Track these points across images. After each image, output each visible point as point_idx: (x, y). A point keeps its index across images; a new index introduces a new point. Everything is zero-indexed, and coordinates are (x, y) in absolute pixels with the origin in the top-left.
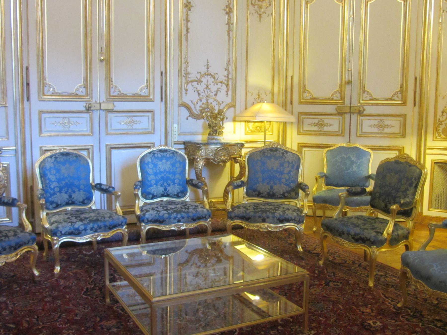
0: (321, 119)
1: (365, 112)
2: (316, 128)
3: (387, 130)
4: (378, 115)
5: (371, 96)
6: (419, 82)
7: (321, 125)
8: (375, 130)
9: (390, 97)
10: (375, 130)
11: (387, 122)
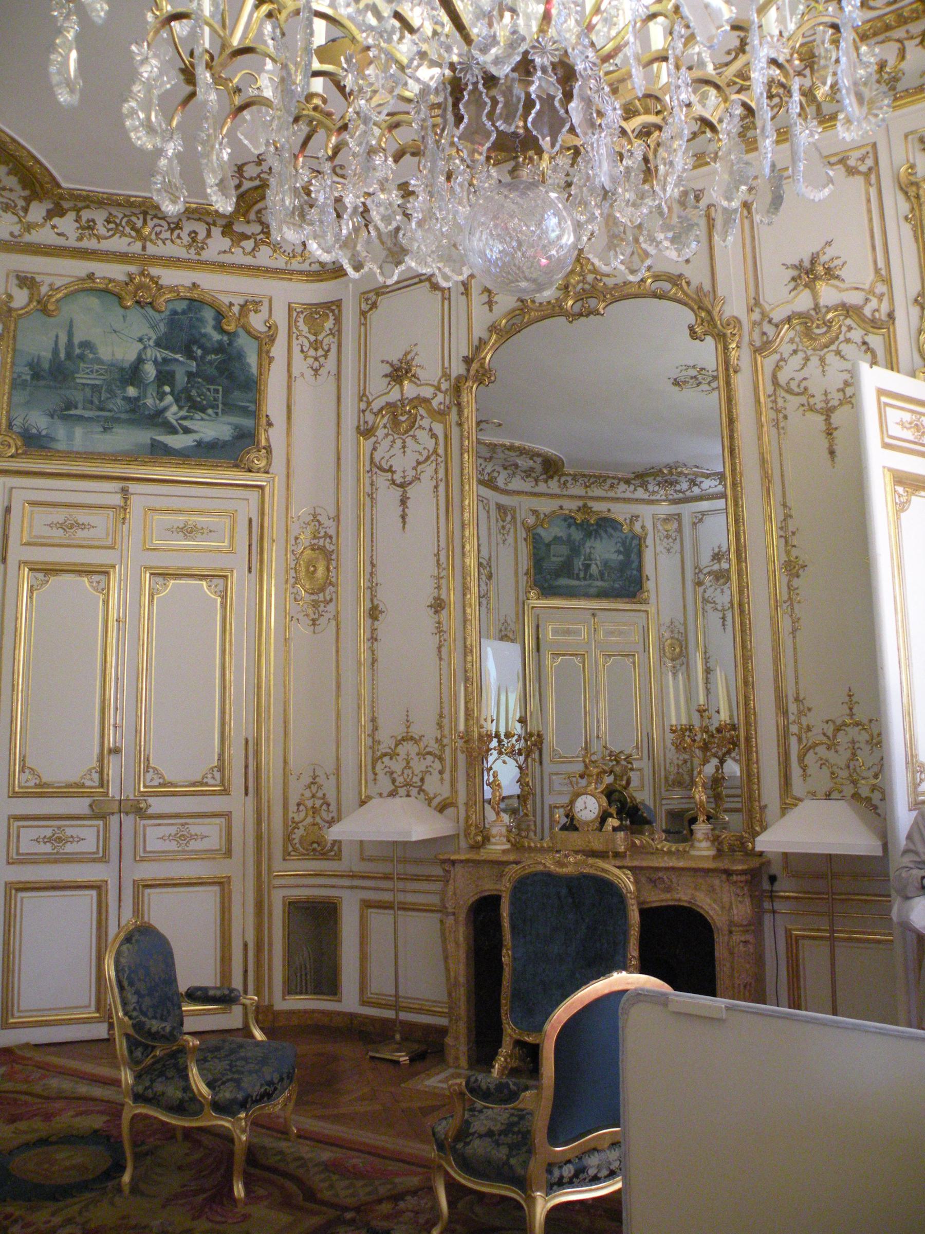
0: (59, 828)
1: (150, 811)
2: (47, 848)
3: (194, 845)
4: (177, 816)
5: (162, 777)
6: (252, 748)
7: (59, 839)
8: (173, 846)
9: (199, 778)
10: (173, 846)
11: (194, 830)
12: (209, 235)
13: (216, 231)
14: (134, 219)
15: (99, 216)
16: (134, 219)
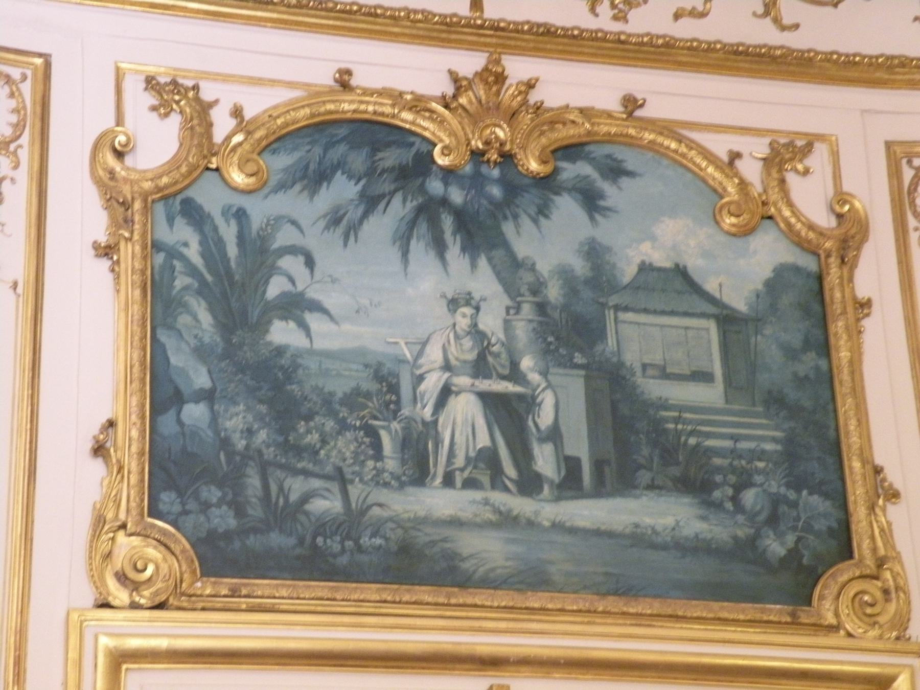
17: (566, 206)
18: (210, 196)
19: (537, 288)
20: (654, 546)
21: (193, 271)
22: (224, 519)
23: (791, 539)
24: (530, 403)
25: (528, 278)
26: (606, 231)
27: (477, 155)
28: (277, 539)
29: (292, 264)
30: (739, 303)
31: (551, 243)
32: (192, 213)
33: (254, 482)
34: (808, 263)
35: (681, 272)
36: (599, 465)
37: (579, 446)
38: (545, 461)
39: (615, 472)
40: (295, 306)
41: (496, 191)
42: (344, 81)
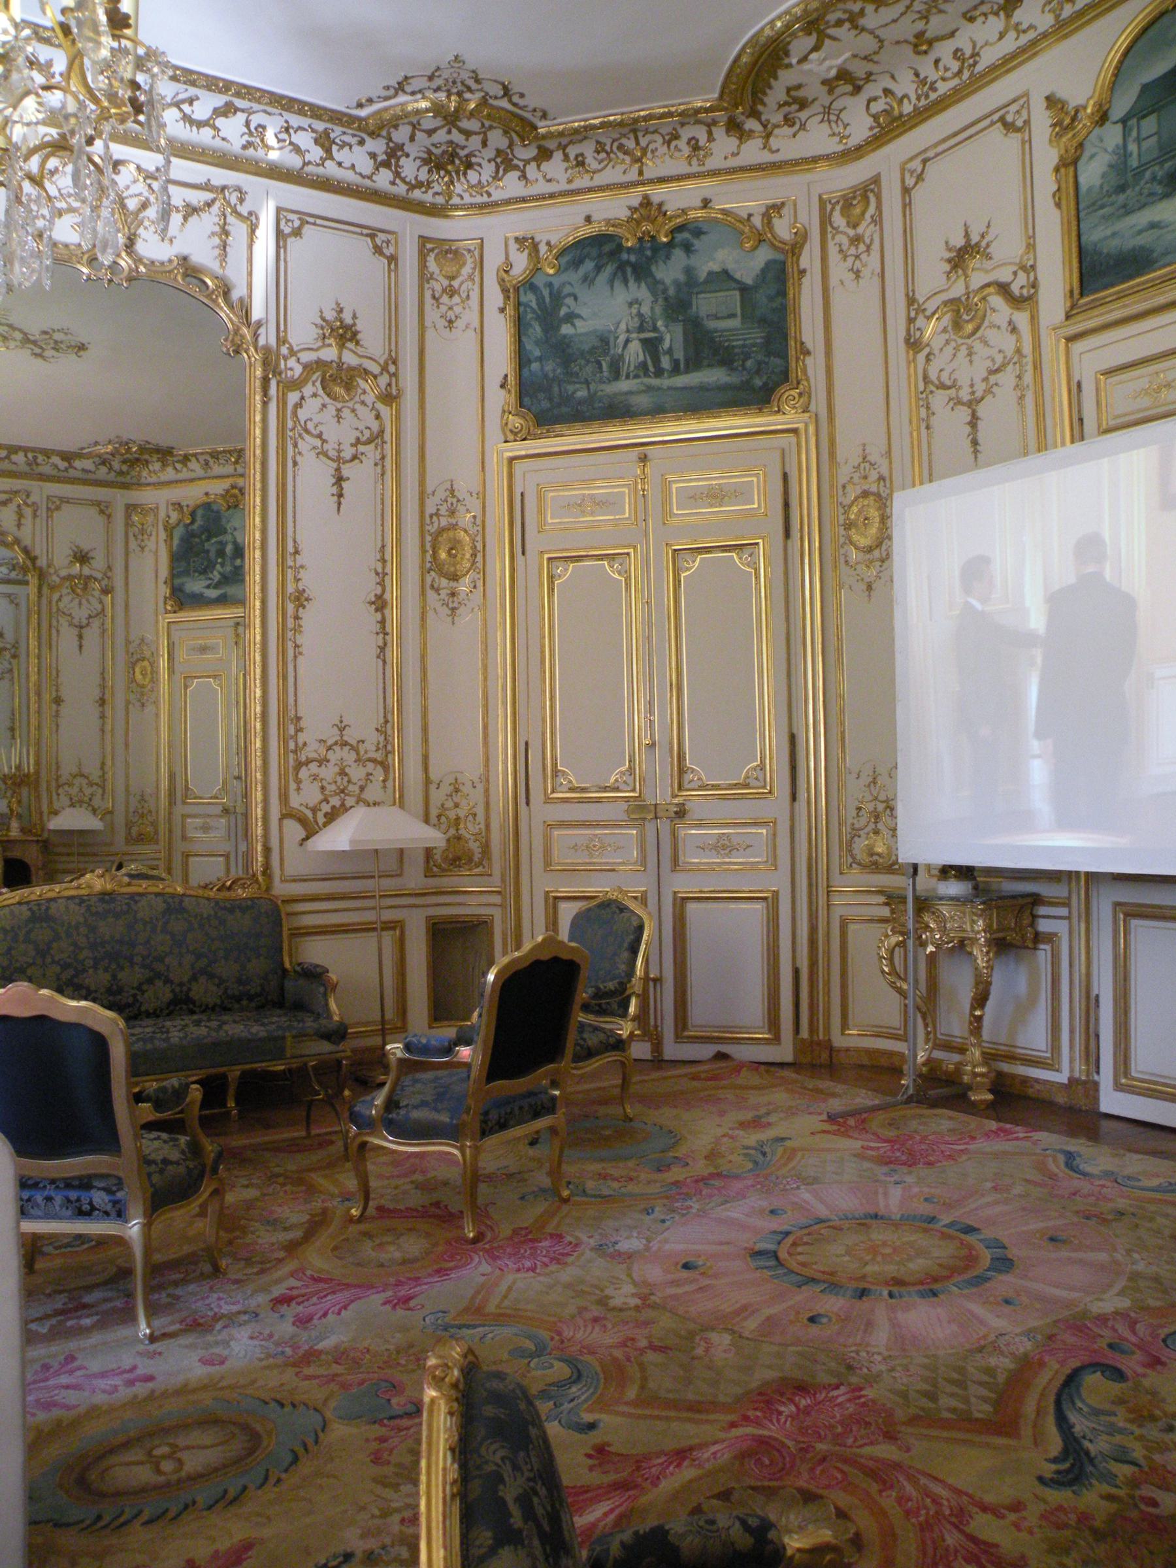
12: (710, 138)
13: (719, 132)
14: (624, 141)
15: (588, 148)
16: (624, 141)
17: (678, 253)
18: (539, 281)
19: (665, 291)
20: (708, 390)
21: (534, 311)
22: (545, 404)
23: (765, 378)
24: (660, 340)
25: (661, 287)
26: (694, 261)
27: (640, 239)
28: (564, 410)
29: (569, 301)
30: (749, 281)
31: (669, 272)
32: (533, 288)
33: (556, 389)
34: (781, 257)
35: (725, 272)
36: (687, 361)
37: (679, 355)
38: (666, 363)
39: (694, 363)
40: (571, 318)
41: (649, 253)
42: (588, 219)
